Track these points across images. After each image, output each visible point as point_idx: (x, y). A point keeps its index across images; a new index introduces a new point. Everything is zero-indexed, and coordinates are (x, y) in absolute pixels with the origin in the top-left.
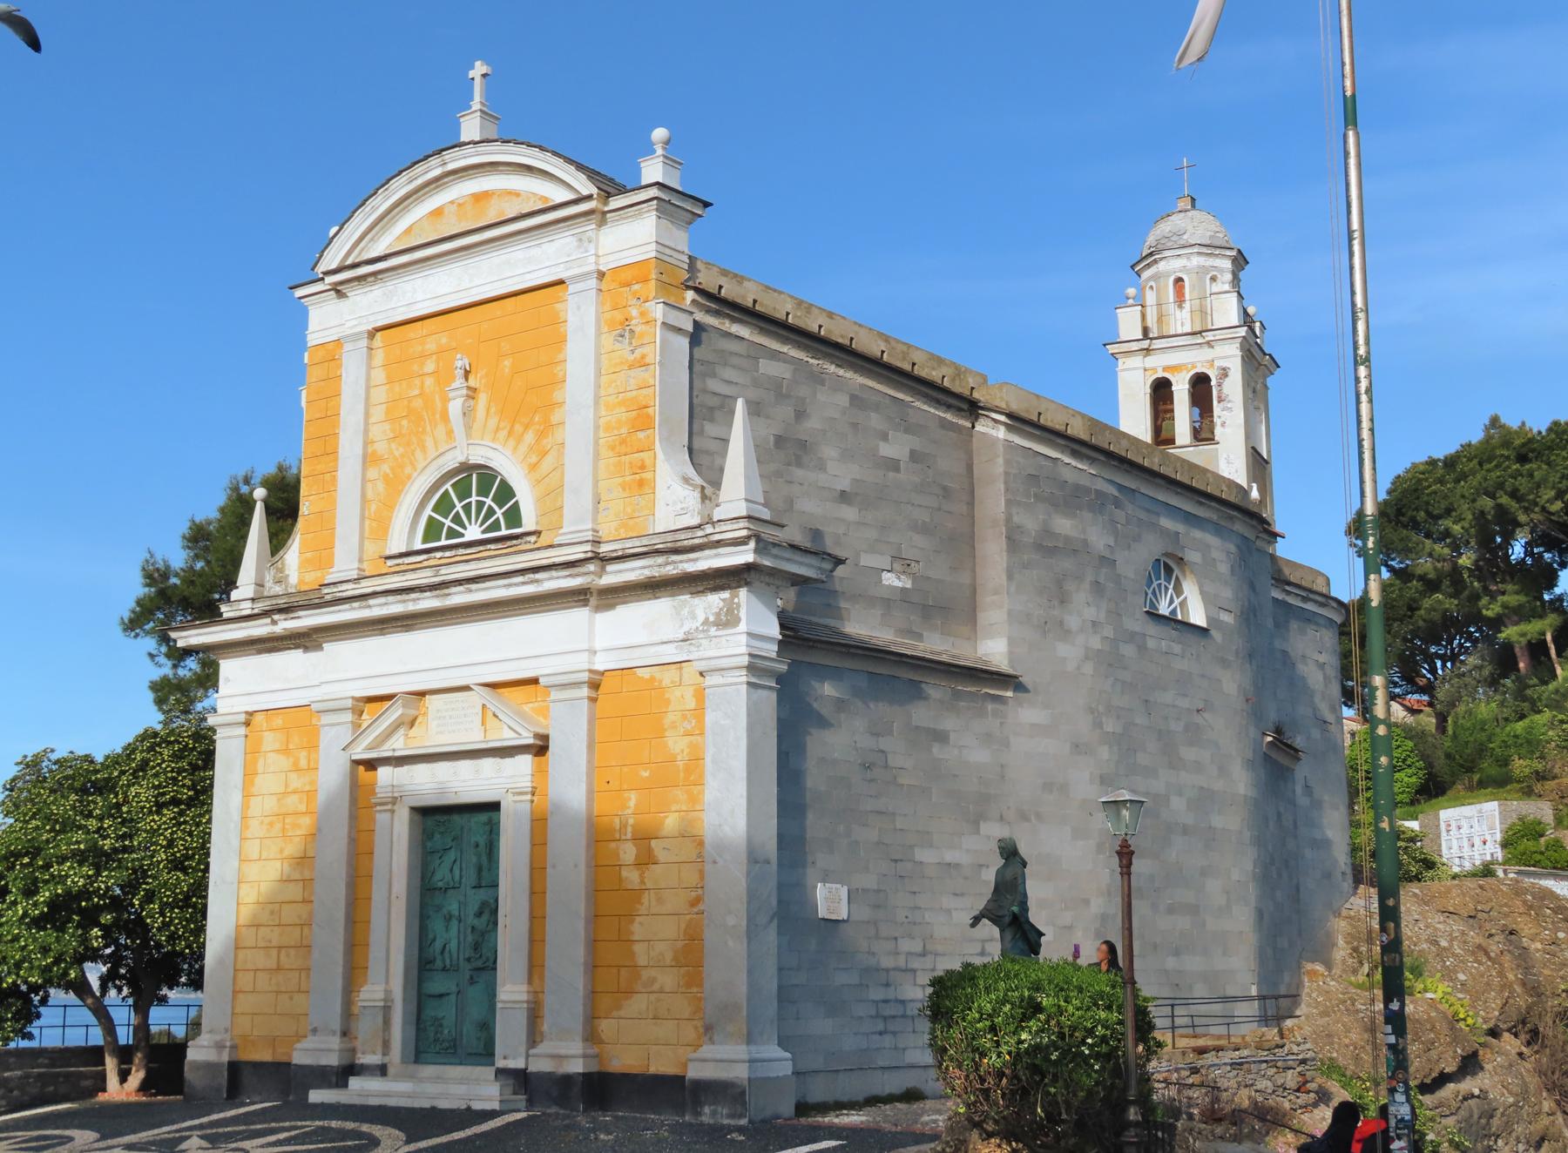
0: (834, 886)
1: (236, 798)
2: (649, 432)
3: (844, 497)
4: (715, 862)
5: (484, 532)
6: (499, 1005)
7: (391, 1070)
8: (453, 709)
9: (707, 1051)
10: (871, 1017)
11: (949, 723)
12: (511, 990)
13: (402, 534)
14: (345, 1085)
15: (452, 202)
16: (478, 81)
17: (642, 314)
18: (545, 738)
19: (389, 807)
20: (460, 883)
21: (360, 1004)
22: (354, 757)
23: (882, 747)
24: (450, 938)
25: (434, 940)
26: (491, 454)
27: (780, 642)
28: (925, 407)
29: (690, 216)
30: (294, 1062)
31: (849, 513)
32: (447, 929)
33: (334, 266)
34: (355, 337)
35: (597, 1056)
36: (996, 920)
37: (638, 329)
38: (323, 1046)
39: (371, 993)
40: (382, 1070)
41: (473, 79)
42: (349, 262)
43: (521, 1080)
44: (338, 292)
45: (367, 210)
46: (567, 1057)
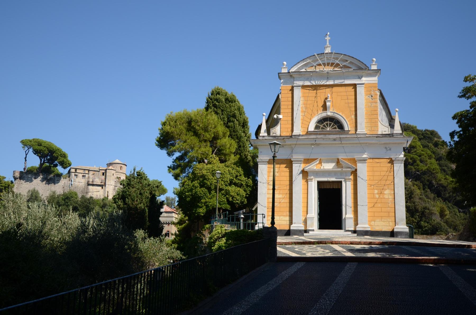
4: (397, 194)
5: (331, 129)
37: (373, 96)
40: (313, 230)
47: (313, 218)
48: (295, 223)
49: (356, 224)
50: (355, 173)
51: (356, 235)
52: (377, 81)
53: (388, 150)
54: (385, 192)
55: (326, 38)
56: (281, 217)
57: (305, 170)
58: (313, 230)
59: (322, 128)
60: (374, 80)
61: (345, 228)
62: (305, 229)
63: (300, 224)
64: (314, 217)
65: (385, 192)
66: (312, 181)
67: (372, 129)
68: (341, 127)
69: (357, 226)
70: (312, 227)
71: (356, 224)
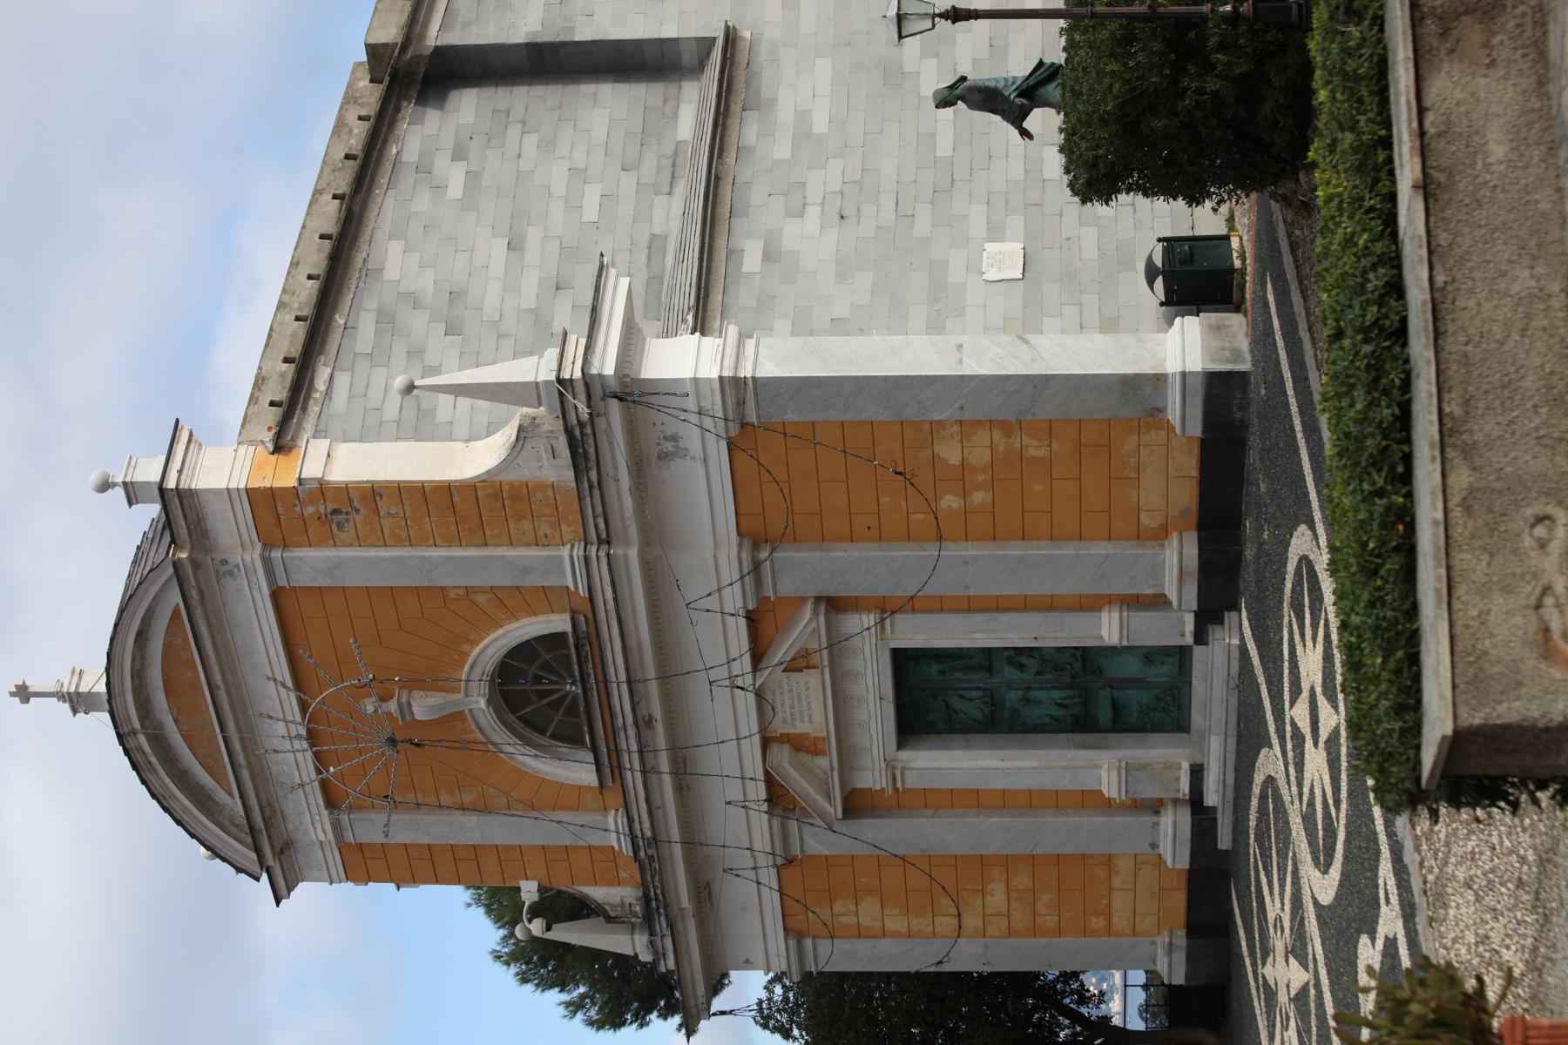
0: (985, 261)
1: (885, 945)
2: (454, 491)
3: (515, 246)
4: (962, 408)
6: (1125, 643)
7: (1198, 759)
8: (783, 705)
10: (1135, 211)
11: (785, 110)
12: (1108, 629)
14: (1214, 809)
15: (176, 721)
17: (312, 502)
18: (818, 600)
19: (898, 773)
20: (985, 689)
21: (1123, 797)
22: (840, 815)
23: (819, 200)
24: (1049, 699)
25: (1051, 717)
26: (478, 672)
27: (703, 334)
28: (1019, 764)
29: (192, 446)
30: (1187, 867)
31: (533, 236)
32: (1038, 703)
33: (254, 856)
34: (337, 827)
35: (1181, 533)
36: (1025, 113)
39: (1109, 784)
40: (1197, 772)
42: (249, 840)
43: (1209, 615)
44: (282, 851)
45: (187, 819)
46: (1181, 568)
53: (677, 447)
54: (955, 460)
56: (1116, 882)
58: (1197, 772)
65: (955, 460)
67: (547, 511)
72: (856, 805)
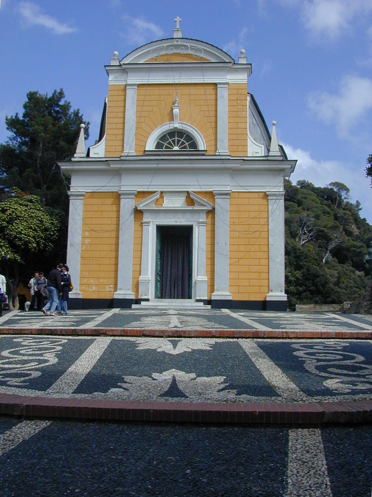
4: (273, 245)
5: (180, 149)
9: (270, 294)
13: (151, 145)
14: (140, 304)
16: (178, 22)
38: (126, 293)
40: (148, 300)
41: (176, 21)
47: (147, 282)
48: (120, 289)
49: (212, 288)
50: (211, 212)
51: (209, 307)
52: (247, 80)
55: (175, 20)
57: (138, 208)
58: (148, 300)
59: (167, 147)
60: (241, 78)
61: (195, 296)
62: (137, 298)
63: (128, 290)
64: (150, 280)
66: (149, 225)
68: (194, 145)
69: (213, 292)
70: (146, 295)
71: (212, 288)
72: (138, 213)
